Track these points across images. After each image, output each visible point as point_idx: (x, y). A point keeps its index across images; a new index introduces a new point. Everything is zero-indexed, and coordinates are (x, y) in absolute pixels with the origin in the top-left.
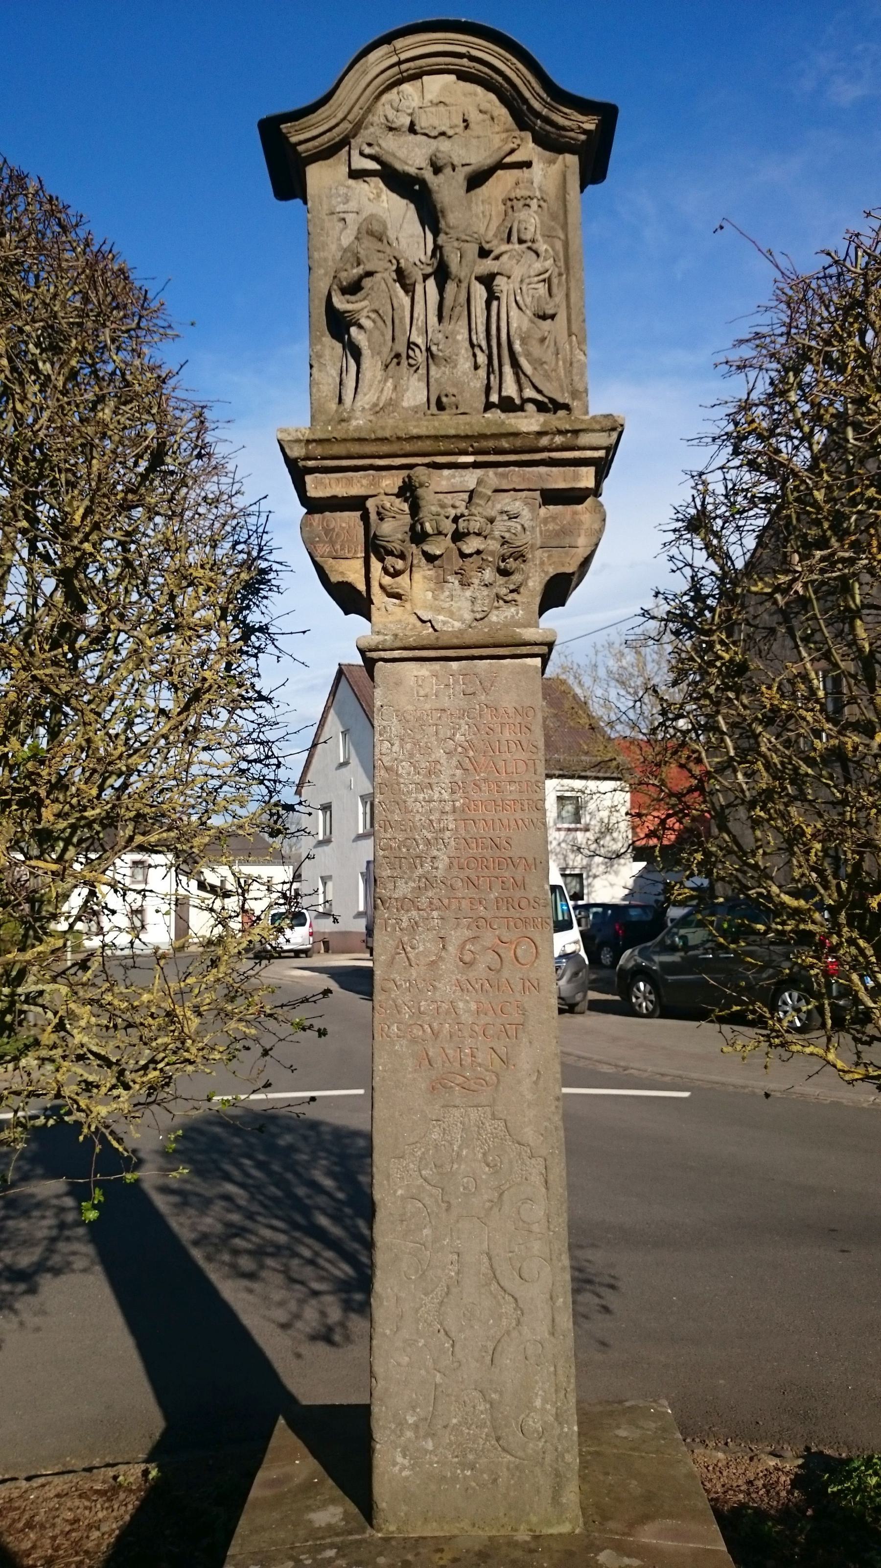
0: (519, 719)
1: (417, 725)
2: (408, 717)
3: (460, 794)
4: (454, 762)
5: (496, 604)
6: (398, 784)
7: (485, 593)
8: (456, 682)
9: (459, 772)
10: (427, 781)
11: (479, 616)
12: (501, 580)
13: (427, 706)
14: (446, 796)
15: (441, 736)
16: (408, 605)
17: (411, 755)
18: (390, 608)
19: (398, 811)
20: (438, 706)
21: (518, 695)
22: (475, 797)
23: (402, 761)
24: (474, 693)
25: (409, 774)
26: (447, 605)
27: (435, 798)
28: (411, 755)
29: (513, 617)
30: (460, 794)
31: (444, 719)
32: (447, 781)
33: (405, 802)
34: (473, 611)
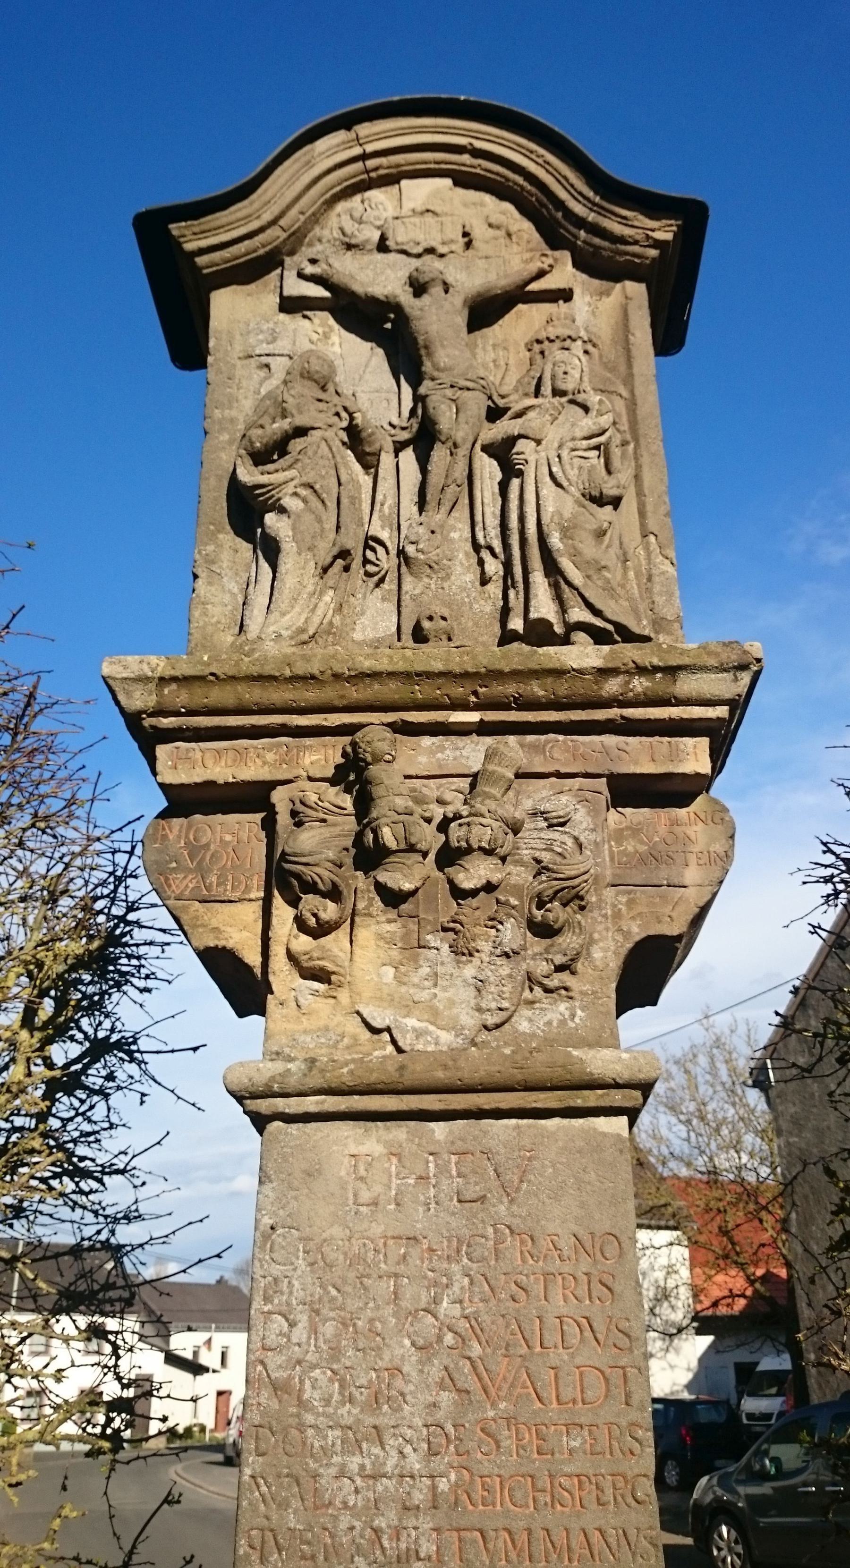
0: (585, 1264)
1: (352, 1275)
2: (332, 1256)
3: (449, 1456)
4: (435, 1372)
5: (527, 994)
6: (301, 1427)
7: (505, 971)
8: (443, 1170)
9: (446, 1398)
10: (370, 1420)
11: (491, 1020)
12: (537, 945)
13: (377, 1230)
14: (415, 1462)
15: (406, 1304)
16: (344, 996)
17: (336, 1353)
18: (307, 1000)
19: (296, 1503)
20: (401, 1230)
21: (582, 1205)
22: (486, 1468)
23: (313, 1367)
24: (482, 1199)
25: (327, 1401)
26: (424, 995)
27: (388, 1468)
28: (336, 1353)
29: (563, 1022)
30: (449, 1456)
31: (414, 1260)
32: (418, 1422)
33: (315, 1476)
34: (479, 1010)
